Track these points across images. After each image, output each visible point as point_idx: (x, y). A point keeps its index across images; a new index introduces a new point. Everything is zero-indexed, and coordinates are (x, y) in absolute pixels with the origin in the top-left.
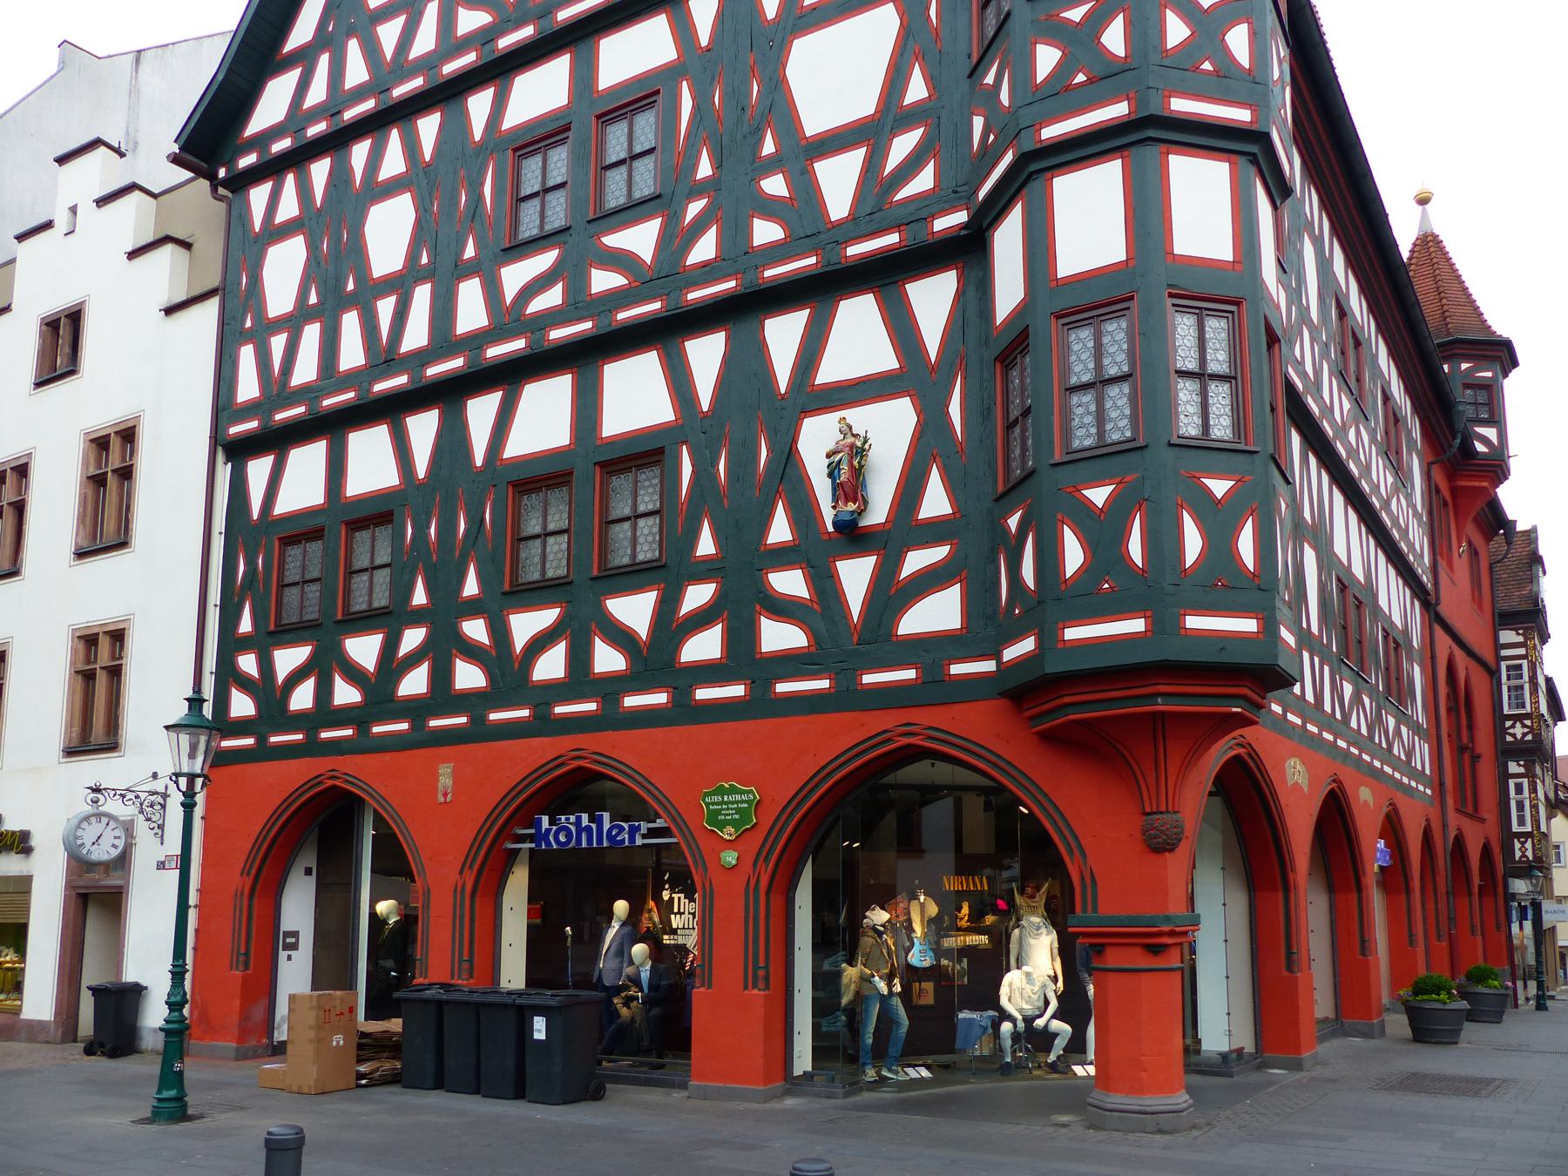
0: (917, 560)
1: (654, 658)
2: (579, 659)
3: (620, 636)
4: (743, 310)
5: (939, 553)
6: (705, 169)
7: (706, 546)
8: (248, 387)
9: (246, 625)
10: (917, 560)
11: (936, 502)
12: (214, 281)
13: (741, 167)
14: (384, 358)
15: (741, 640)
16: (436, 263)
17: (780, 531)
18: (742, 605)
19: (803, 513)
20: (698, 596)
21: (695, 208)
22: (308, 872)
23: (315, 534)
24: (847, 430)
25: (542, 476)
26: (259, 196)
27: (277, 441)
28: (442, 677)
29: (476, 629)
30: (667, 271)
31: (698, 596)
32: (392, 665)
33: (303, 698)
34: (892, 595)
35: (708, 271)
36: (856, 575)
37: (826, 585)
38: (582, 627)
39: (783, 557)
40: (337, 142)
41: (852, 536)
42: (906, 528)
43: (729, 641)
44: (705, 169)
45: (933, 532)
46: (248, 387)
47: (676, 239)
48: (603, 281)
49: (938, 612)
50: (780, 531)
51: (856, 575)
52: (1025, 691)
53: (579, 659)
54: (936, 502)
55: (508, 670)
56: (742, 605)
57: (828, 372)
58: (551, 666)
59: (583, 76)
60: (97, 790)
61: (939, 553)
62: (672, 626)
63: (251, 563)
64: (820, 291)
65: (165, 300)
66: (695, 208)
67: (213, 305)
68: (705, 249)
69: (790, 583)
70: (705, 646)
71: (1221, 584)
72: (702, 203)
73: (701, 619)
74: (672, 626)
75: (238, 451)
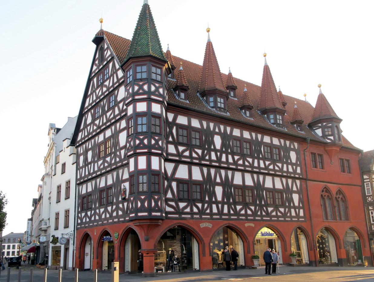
4: (117, 168)
8: (79, 177)
9: (79, 210)
12: (75, 161)
14: (89, 174)
21: (113, 155)
25: (102, 190)
26: (79, 149)
27: (81, 183)
46: (79, 177)
57: (124, 178)
65: (72, 163)
66: (113, 155)
67: (76, 164)
75: (79, 184)
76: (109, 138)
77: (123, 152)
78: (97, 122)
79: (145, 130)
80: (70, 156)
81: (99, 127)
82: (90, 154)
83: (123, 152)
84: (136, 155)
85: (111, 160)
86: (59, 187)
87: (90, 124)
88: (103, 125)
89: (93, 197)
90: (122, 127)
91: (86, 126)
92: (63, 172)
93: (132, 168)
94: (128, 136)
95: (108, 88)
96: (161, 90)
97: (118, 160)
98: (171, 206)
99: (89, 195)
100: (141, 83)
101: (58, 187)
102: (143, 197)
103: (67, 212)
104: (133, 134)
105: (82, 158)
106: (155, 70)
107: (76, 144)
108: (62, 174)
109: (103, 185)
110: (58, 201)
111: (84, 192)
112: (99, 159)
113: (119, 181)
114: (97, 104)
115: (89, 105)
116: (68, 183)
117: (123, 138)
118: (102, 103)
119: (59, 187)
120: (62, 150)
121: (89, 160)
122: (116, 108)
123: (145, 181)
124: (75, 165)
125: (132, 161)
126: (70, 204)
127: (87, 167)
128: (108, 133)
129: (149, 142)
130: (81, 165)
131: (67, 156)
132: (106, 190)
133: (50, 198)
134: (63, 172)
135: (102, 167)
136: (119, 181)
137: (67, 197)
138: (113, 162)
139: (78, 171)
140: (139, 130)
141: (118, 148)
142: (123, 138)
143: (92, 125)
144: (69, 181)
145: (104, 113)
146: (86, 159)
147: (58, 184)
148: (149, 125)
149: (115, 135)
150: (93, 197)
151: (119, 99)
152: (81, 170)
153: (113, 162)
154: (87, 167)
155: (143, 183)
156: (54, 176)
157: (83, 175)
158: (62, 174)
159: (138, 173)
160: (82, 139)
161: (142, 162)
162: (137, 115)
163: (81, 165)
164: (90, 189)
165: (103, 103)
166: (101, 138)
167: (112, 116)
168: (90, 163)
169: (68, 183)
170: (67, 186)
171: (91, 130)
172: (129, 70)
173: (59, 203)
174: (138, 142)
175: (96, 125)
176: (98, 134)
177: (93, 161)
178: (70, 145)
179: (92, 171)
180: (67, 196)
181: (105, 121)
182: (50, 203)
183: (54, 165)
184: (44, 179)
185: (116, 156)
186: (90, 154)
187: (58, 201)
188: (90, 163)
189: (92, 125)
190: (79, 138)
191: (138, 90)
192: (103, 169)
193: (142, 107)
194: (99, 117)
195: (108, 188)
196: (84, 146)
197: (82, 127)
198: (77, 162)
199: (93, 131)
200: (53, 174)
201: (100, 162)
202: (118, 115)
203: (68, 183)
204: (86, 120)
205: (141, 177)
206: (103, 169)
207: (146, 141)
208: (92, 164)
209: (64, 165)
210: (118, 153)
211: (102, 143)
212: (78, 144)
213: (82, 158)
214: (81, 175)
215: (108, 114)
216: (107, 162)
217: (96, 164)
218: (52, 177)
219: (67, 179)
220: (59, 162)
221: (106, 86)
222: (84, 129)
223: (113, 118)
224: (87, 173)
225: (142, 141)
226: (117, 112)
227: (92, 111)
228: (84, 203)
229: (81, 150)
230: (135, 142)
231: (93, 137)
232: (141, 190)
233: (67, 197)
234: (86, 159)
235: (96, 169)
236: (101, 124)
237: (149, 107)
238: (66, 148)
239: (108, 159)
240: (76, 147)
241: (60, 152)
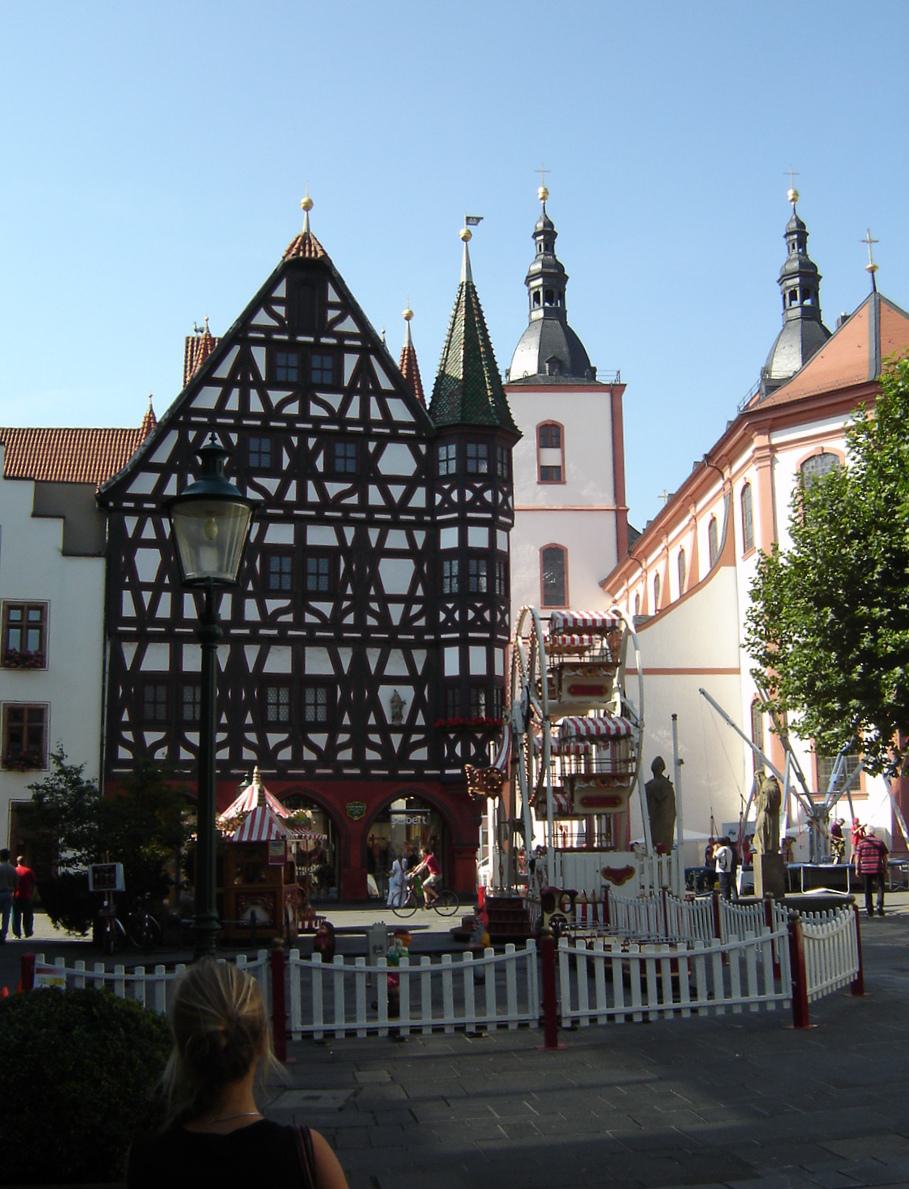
0: (415, 738)
1: (327, 756)
2: (297, 753)
3: (314, 748)
5: (421, 737)
6: (349, 591)
7: (346, 721)
10: (415, 738)
11: (420, 721)
15: (359, 755)
17: (372, 721)
18: (359, 743)
19: (380, 715)
20: (343, 738)
21: (346, 604)
29: (252, 737)
30: (334, 622)
31: (343, 738)
34: (408, 748)
36: (396, 739)
38: (298, 741)
39: (373, 730)
42: (409, 729)
43: (354, 753)
44: (349, 591)
45: (419, 730)
47: (339, 614)
48: (309, 618)
49: (420, 754)
50: (372, 721)
51: (396, 739)
53: (297, 753)
54: (420, 721)
56: (359, 743)
59: (300, 535)
61: (421, 737)
62: (333, 747)
68: (349, 619)
69: (375, 738)
70: (346, 755)
72: (348, 603)
73: (344, 746)
74: (333, 747)
90: (389, 544)
141: (372, 592)
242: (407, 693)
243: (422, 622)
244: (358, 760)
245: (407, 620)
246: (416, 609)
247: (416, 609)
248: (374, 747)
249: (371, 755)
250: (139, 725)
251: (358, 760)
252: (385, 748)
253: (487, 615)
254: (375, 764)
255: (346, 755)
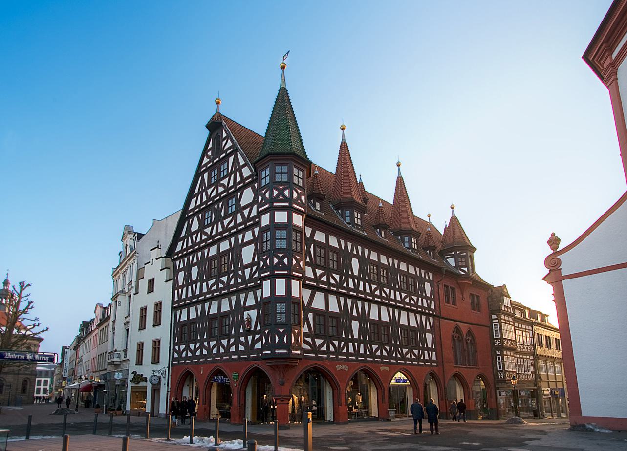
0: (257, 336)
2: (218, 350)
4: (238, 292)
8: (176, 299)
9: (177, 341)
11: (259, 328)
13: (237, 269)
15: (237, 348)
16: (200, 280)
17: (242, 331)
18: (237, 343)
21: (231, 275)
22: (188, 385)
23: (186, 325)
24: (248, 314)
25: (214, 317)
27: (181, 308)
28: (202, 352)
32: (196, 350)
33: (184, 355)
34: (254, 342)
35: (233, 286)
36: (250, 338)
37: (246, 339)
40: (188, 254)
41: (248, 332)
46: (176, 299)
48: (221, 286)
51: (250, 338)
52: (266, 358)
53: (218, 350)
54: (259, 328)
55: (210, 350)
58: (215, 351)
60: (154, 371)
63: (177, 330)
64: (247, 290)
65: (165, 279)
66: (231, 275)
67: (172, 281)
71: (281, 345)
74: (229, 346)
76: (226, 252)
77: (247, 271)
78: (208, 230)
79: (284, 246)
80: (161, 270)
81: (210, 237)
82: (195, 271)
83: (247, 271)
84: (273, 278)
85: (229, 280)
86: (144, 310)
87: (196, 232)
88: (217, 234)
89: (199, 326)
91: (189, 233)
92: (151, 289)
93: (267, 293)
94: (258, 253)
95: (227, 189)
96: (303, 198)
97: (239, 280)
98: (307, 343)
99: (190, 322)
100: (281, 187)
101: (142, 309)
102: (281, 331)
103: (157, 344)
104: (269, 250)
105: (181, 275)
106: (297, 172)
107: (174, 257)
108: (148, 293)
109: (214, 310)
110: (142, 327)
111: (184, 318)
112: (210, 278)
113: (240, 309)
114: (207, 207)
115: (196, 207)
116: (159, 305)
117: (248, 254)
118: (216, 206)
119: (144, 310)
120: (149, 262)
121: (194, 278)
122: (239, 215)
123: (284, 310)
124: (172, 281)
125: (267, 284)
126: (164, 333)
127: (190, 287)
128: (225, 246)
129: (290, 262)
130: (180, 284)
131: (156, 270)
132: (219, 319)
133: (127, 323)
134: (151, 289)
135: (214, 288)
136: (240, 309)
137: (157, 323)
138: (232, 282)
139: (176, 291)
140: (278, 246)
142: (248, 254)
143: (199, 233)
144: (161, 304)
145: (219, 219)
146: (188, 276)
147: (143, 306)
148: (289, 239)
149: (237, 249)
150: (199, 326)
151: (243, 204)
152: (180, 290)
153: (232, 282)
154: (190, 287)
155: (281, 313)
156: (134, 294)
157: (184, 296)
158: (148, 293)
159: (274, 298)
160: (182, 250)
161: (281, 287)
162: (274, 226)
163: (180, 284)
164: (193, 315)
165: (218, 206)
166: (213, 251)
167: (232, 224)
168: (196, 282)
169: (158, 306)
170: (157, 309)
171: (198, 240)
172: (265, 169)
173: (143, 331)
174: (276, 261)
175: (206, 234)
176: (208, 246)
177: (200, 280)
178: (165, 257)
179: (198, 292)
180: (156, 323)
181: (220, 229)
182: (127, 330)
183: (134, 280)
184: (116, 297)
185: (236, 276)
186: (195, 271)
187: (142, 327)
188: (196, 282)
189: (199, 233)
190: (178, 249)
191: (278, 195)
192: (215, 291)
193: (281, 217)
194: (211, 225)
195: (221, 316)
196: (186, 259)
197: (183, 235)
198: (174, 279)
199: (202, 241)
200: (133, 291)
201: (211, 283)
202: (241, 224)
203: (158, 306)
204: (189, 226)
205: (278, 305)
206: (215, 291)
207: (286, 261)
208: (199, 284)
209: (151, 282)
210: (240, 272)
211: (214, 257)
212: (176, 257)
213: (181, 275)
214: (180, 297)
215: (226, 222)
216: (223, 282)
217: (205, 284)
218: (130, 296)
219: (157, 300)
220: (143, 278)
221: (223, 185)
222: (186, 237)
223: (232, 228)
224: (190, 295)
225: (281, 260)
226: (239, 219)
227: (200, 215)
228: (183, 332)
229: (180, 264)
230: (272, 261)
231: (201, 249)
232: (278, 321)
233: (157, 323)
234: (188, 276)
235: (205, 290)
236: (214, 233)
237: (290, 218)
238: (155, 260)
239: (224, 279)
240: (172, 260)
241: (145, 264)
242: (253, 313)
243: (256, 275)
244: (237, 351)
245: (251, 275)
246: (255, 268)
247: (255, 268)
248: (242, 344)
249: (241, 348)
250: (179, 345)
251: (237, 351)
252: (245, 344)
253: (286, 261)
254: (243, 352)
255: (233, 349)
